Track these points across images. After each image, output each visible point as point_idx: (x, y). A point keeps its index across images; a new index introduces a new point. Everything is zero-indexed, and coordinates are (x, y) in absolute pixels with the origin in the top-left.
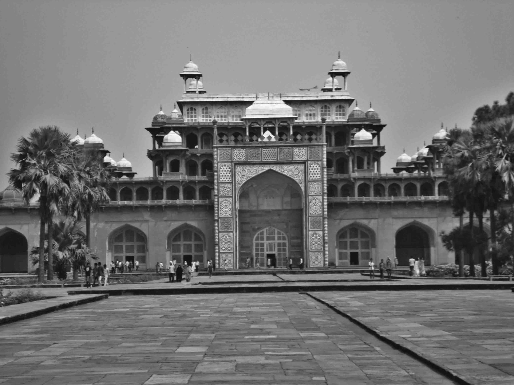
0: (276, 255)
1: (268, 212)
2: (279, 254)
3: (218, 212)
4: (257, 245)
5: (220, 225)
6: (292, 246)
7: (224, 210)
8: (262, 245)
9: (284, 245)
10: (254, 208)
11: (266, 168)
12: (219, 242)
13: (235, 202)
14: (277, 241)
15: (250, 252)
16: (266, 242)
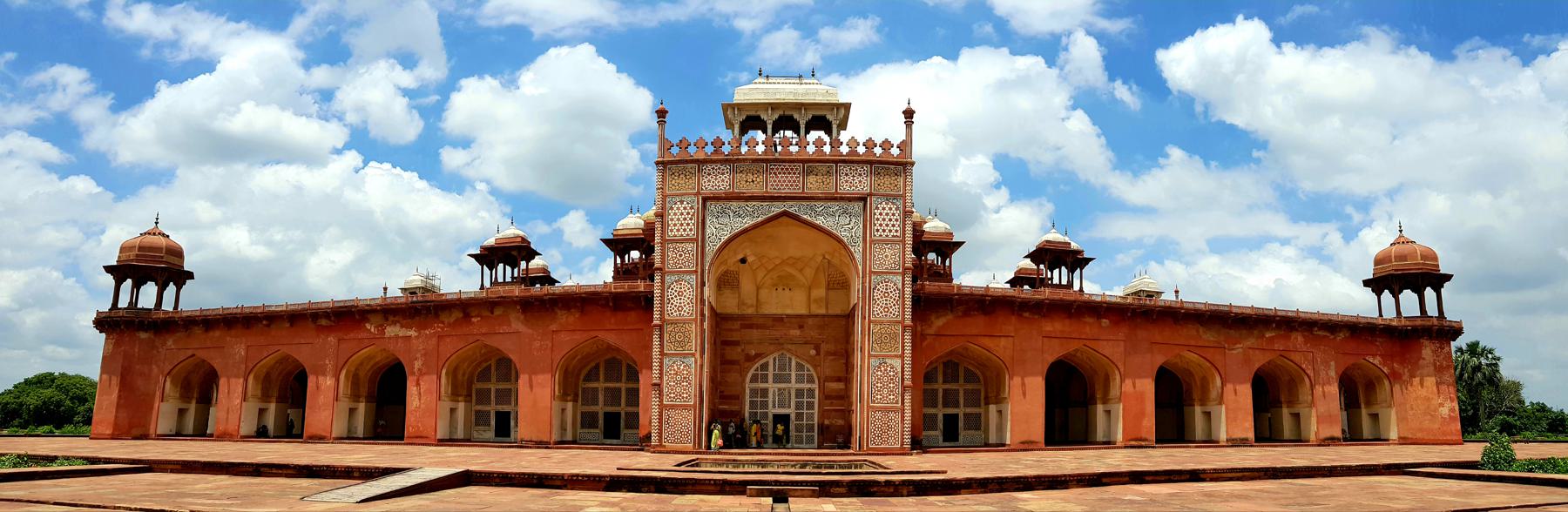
0: (793, 417)
1: (779, 320)
2: (799, 416)
3: (662, 307)
4: (754, 392)
5: (666, 337)
6: (827, 397)
7: (676, 302)
8: (765, 392)
9: (811, 392)
10: (750, 311)
11: (777, 208)
12: (661, 378)
13: (703, 284)
14: (794, 385)
15: (735, 408)
16: (772, 387)
